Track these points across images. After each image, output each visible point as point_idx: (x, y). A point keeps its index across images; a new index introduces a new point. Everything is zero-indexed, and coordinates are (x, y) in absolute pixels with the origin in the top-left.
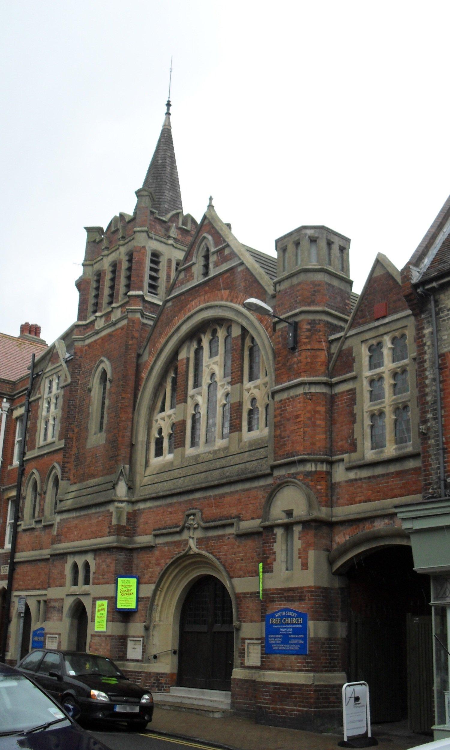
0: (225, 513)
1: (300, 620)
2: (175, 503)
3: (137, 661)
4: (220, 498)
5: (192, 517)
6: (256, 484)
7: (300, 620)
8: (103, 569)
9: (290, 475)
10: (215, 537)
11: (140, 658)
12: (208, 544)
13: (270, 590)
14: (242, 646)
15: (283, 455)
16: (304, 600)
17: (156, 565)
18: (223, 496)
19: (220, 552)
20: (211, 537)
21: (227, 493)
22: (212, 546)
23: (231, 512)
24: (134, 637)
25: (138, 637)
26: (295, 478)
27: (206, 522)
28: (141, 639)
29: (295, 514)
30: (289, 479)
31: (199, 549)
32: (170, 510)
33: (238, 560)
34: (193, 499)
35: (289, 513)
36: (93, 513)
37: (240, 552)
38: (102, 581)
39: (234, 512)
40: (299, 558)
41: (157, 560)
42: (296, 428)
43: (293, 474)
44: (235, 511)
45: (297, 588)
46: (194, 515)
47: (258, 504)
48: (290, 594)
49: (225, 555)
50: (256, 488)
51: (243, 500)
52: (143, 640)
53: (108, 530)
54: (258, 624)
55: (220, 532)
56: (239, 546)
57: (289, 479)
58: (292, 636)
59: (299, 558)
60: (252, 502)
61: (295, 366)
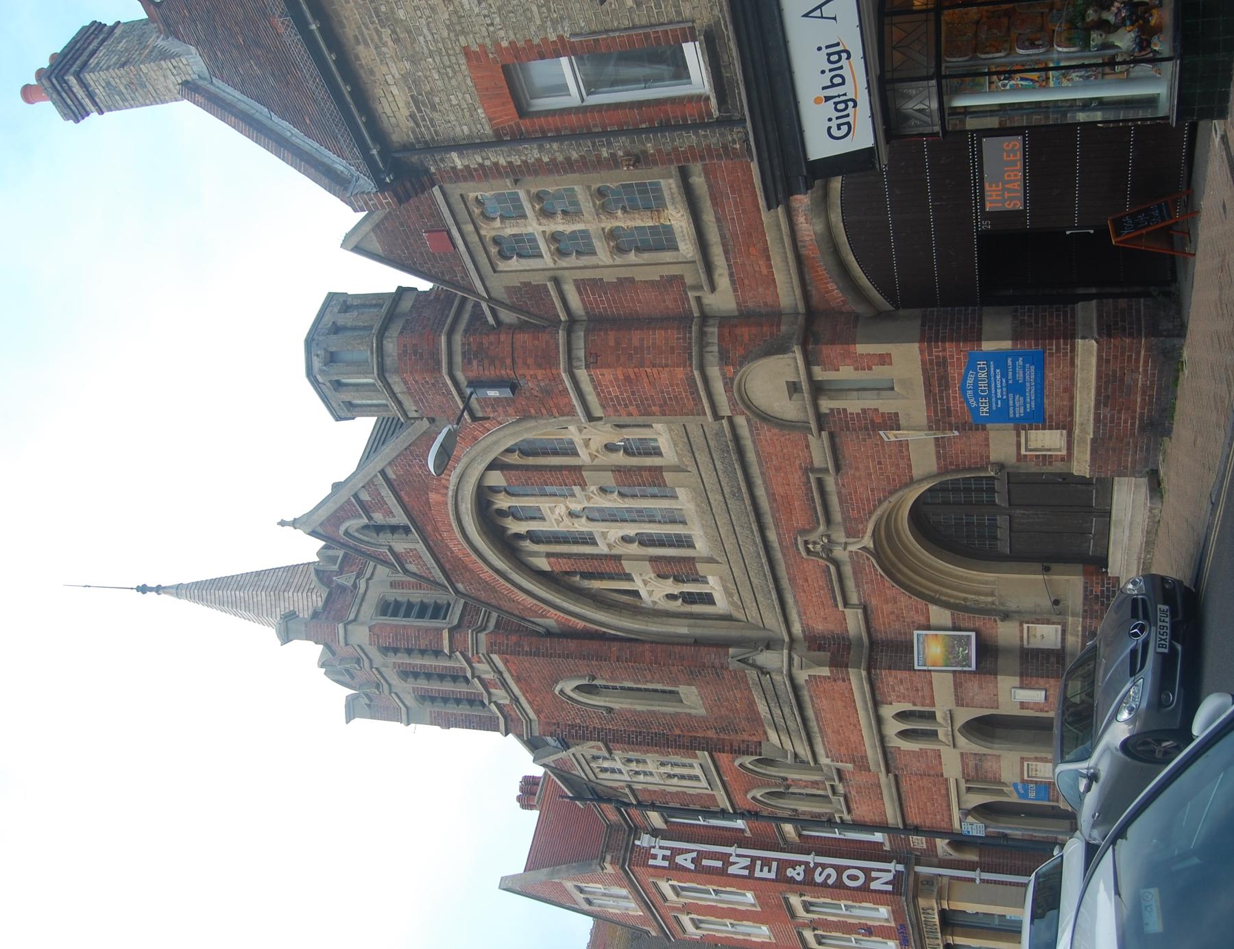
1: (981, 364)
4: (775, 500)
5: (810, 546)
6: (748, 443)
7: (981, 364)
10: (842, 508)
12: (855, 519)
16: (944, 358)
18: (772, 497)
19: (868, 499)
21: (766, 489)
22: (859, 512)
23: (797, 482)
27: (818, 523)
31: (864, 533)
35: (794, 388)
37: (868, 467)
39: (796, 478)
40: (870, 369)
44: (796, 476)
45: (924, 371)
46: (806, 543)
47: (783, 439)
48: (936, 382)
49: (872, 490)
50: (754, 442)
54: (992, 434)
55: (834, 500)
56: (857, 469)
58: (1010, 376)
59: (870, 369)
60: (778, 448)
61: (542, 384)
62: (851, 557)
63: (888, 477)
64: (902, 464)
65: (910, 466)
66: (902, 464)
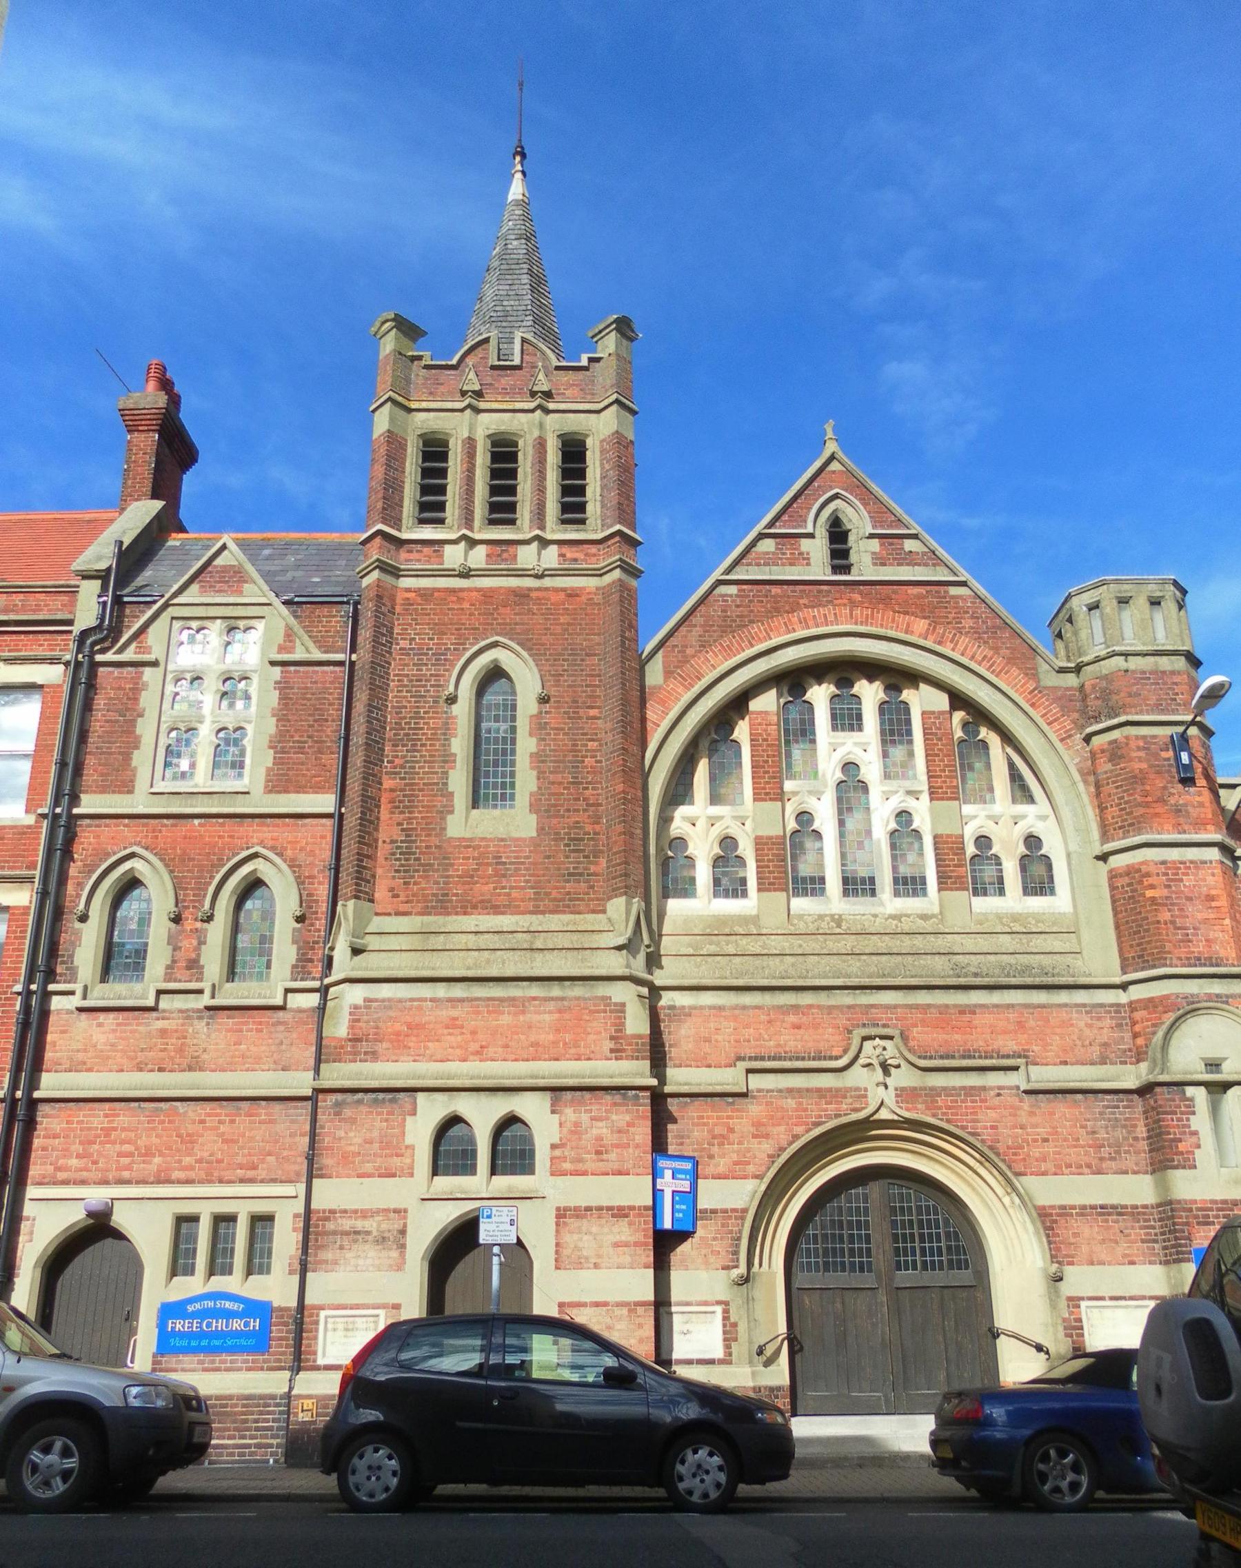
0: (981, 1043)
2: (810, 1006)
3: (711, 1362)
4: (962, 1012)
6: (1063, 997)
8: (599, 1139)
9: (1210, 997)
10: (954, 1088)
11: (719, 1353)
13: (1195, 1202)
14: (1071, 1313)
15: (1188, 959)
17: (755, 1136)
18: (972, 1010)
19: (977, 1121)
20: (944, 1089)
24: (688, 1304)
25: (706, 1303)
26: (1227, 1003)
28: (719, 1309)
29: (1225, 1066)
30: (1219, 1005)
32: (792, 1018)
33: (1035, 1141)
34: (873, 1006)
35: (1213, 1065)
36: (534, 999)
37: (1036, 1126)
38: (590, 1166)
39: (1011, 1045)
41: (758, 1124)
42: (1212, 916)
43: (1217, 996)
49: (992, 1127)
51: (1032, 1023)
52: (726, 1311)
53: (612, 1045)
56: (1032, 1114)
57: (1219, 1005)
62: (858, 1089)
63: (1022, 1148)
64: (1049, 1166)
65: (1044, 1174)
66: (1049, 1166)
